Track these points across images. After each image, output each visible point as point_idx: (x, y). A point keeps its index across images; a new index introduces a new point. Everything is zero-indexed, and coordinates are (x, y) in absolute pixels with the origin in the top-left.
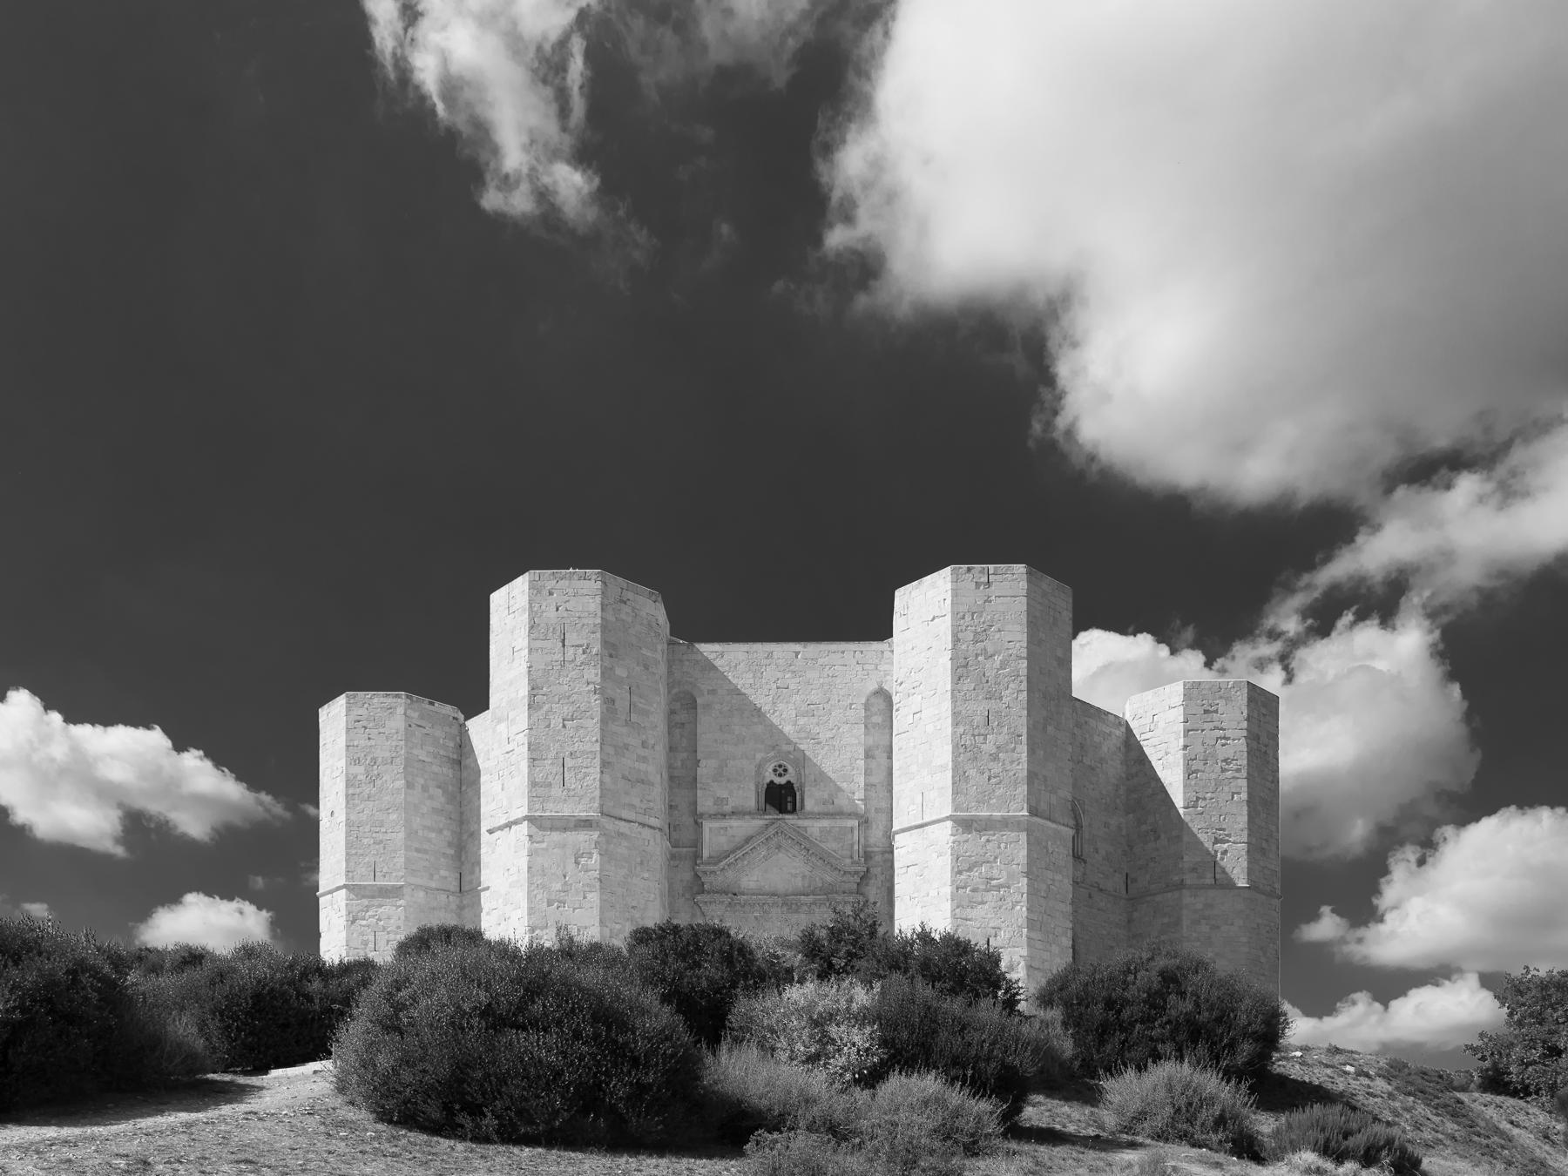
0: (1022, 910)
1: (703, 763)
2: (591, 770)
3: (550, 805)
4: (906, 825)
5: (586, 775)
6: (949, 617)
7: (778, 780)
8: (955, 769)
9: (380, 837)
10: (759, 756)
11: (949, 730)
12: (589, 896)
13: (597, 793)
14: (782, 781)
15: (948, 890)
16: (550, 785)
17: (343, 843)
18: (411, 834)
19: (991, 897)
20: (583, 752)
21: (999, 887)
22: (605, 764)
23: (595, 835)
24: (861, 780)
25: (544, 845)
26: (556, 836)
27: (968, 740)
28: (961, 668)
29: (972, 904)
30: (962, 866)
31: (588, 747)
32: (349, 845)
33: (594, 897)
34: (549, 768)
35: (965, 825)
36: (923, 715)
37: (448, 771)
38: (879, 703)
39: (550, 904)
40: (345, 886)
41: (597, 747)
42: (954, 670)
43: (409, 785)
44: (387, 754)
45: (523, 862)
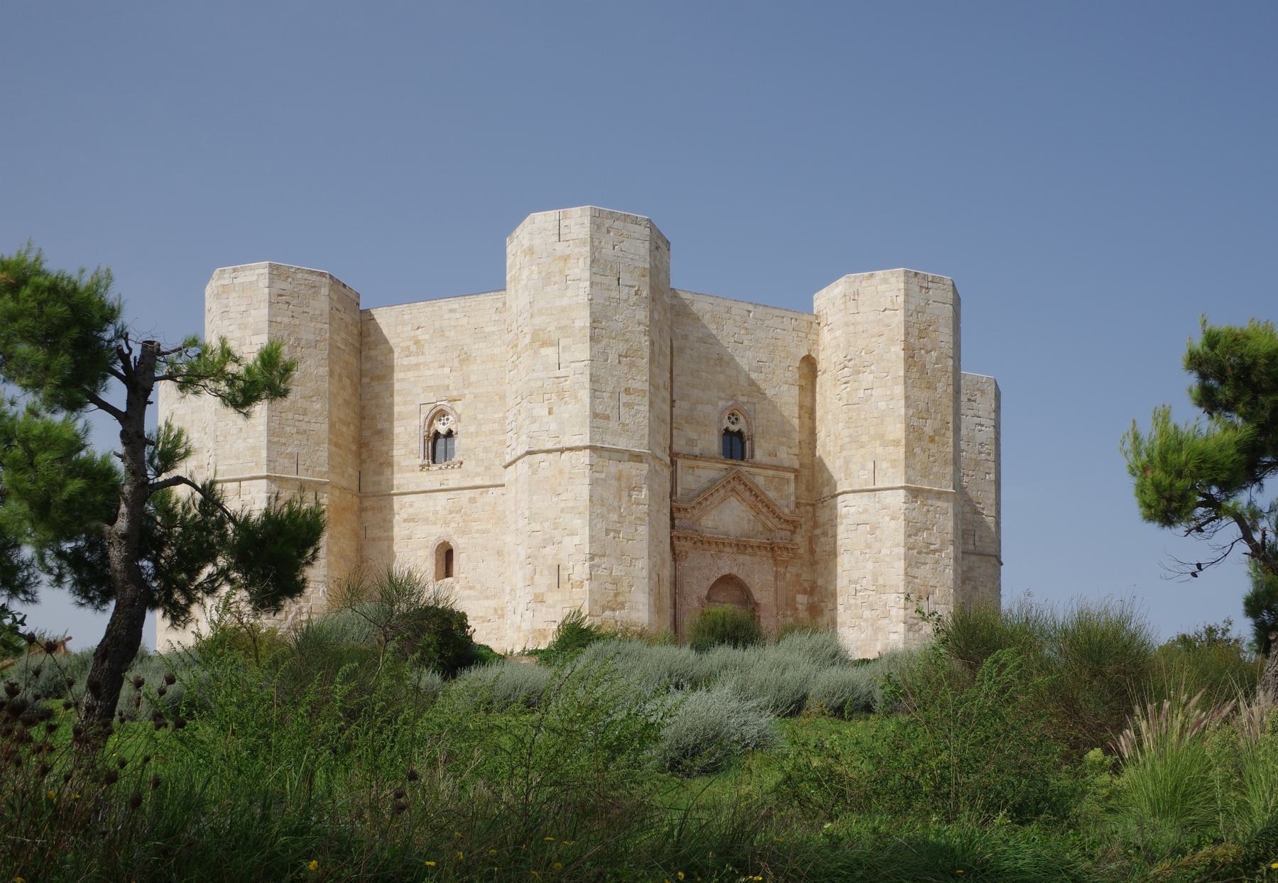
0: (949, 572)
1: (677, 404)
2: (641, 408)
3: (608, 438)
4: (857, 488)
5: (638, 411)
6: (901, 313)
8: (907, 445)
9: (304, 426)
10: (721, 404)
11: (903, 411)
12: (640, 529)
13: (647, 430)
14: (735, 428)
15: (902, 550)
16: (607, 418)
20: (636, 390)
21: (935, 551)
23: (644, 468)
25: (603, 476)
26: (613, 467)
29: (918, 564)
30: (913, 529)
33: (643, 530)
35: (914, 493)
36: (875, 392)
39: (607, 532)
40: (267, 477)
41: (646, 386)
42: (906, 361)
43: (331, 374)
44: (311, 337)
45: (582, 489)
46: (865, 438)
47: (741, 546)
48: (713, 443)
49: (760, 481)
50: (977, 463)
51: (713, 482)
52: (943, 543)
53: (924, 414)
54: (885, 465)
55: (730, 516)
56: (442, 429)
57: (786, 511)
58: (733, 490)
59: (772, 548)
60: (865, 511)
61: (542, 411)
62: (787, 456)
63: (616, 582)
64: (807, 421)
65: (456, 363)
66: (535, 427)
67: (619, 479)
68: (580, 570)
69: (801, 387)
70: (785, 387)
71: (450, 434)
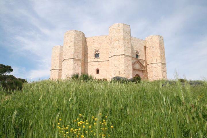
9: (78, 52)
14: (137, 54)
32: (74, 52)
46: (155, 56)
47: (139, 70)
49: (141, 61)
56: (97, 53)
58: (138, 63)
60: (155, 66)
65: (99, 44)
67: (128, 59)
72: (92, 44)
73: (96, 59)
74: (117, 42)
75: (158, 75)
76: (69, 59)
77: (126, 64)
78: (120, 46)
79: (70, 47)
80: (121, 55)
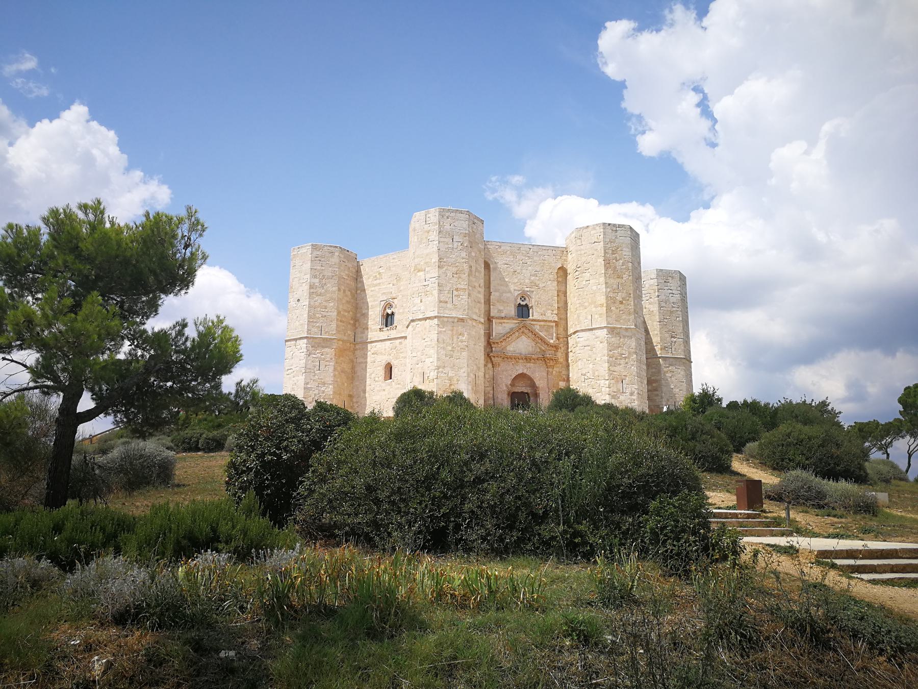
0: (634, 368)
7: (522, 303)
9: (324, 314)
10: (516, 293)
14: (524, 303)
15: (606, 358)
17: (306, 316)
18: (339, 313)
19: (623, 361)
22: (469, 295)
24: (556, 305)
27: (611, 295)
28: (607, 263)
30: (612, 347)
31: (462, 287)
32: (309, 317)
33: (465, 354)
34: (446, 296)
35: (612, 331)
37: (353, 284)
38: (561, 273)
41: (466, 287)
43: (339, 290)
46: (586, 304)
47: (527, 359)
48: (512, 310)
50: (671, 312)
51: (512, 329)
52: (629, 353)
53: (615, 291)
54: (597, 316)
55: (522, 345)
56: (389, 312)
57: (552, 341)
59: (544, 359)
61: (418, 301)
62: (551, 316)
63: (450, 379)
64: (563, 298)
65: (395, 282)
66: (415, 308)
68: (433, 374)
69: (558, 282)
70: (549, 282)
71: (393, 314)
72: (375, 282)
73: (384, 335)
74: (421, 273)
75: (596, 374)
76: (296, 340)
77: (444, 348)
78: (428, 289)
79: (298, 300)
80: (429, 318)
